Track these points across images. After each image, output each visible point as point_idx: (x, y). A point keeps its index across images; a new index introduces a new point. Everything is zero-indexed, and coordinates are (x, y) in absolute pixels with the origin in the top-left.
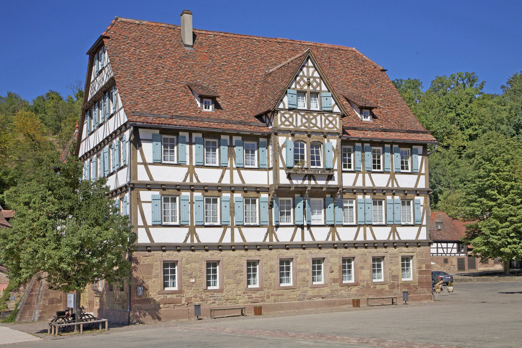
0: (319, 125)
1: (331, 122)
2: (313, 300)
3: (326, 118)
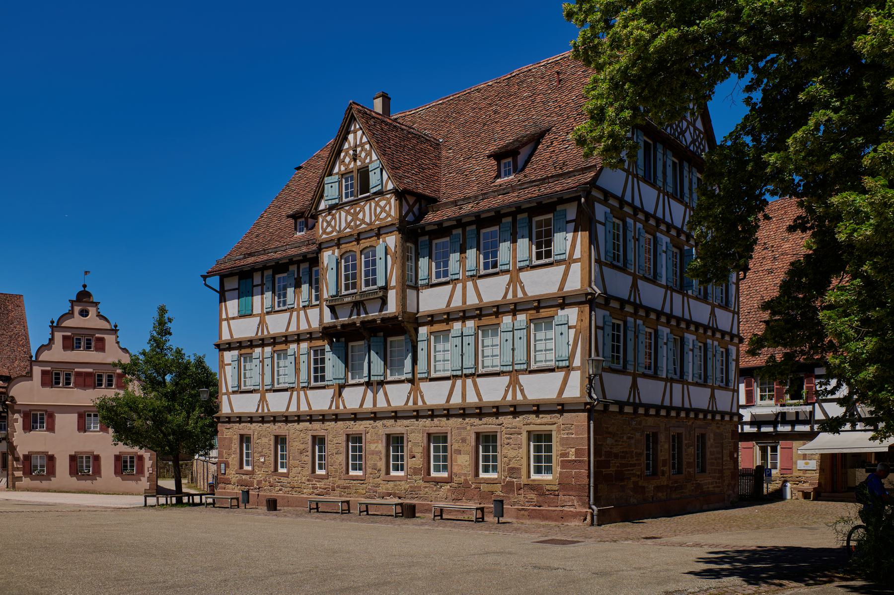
0: (367, 220)
1: (383, 209)
2: (386, 499)
3: (377, 204)
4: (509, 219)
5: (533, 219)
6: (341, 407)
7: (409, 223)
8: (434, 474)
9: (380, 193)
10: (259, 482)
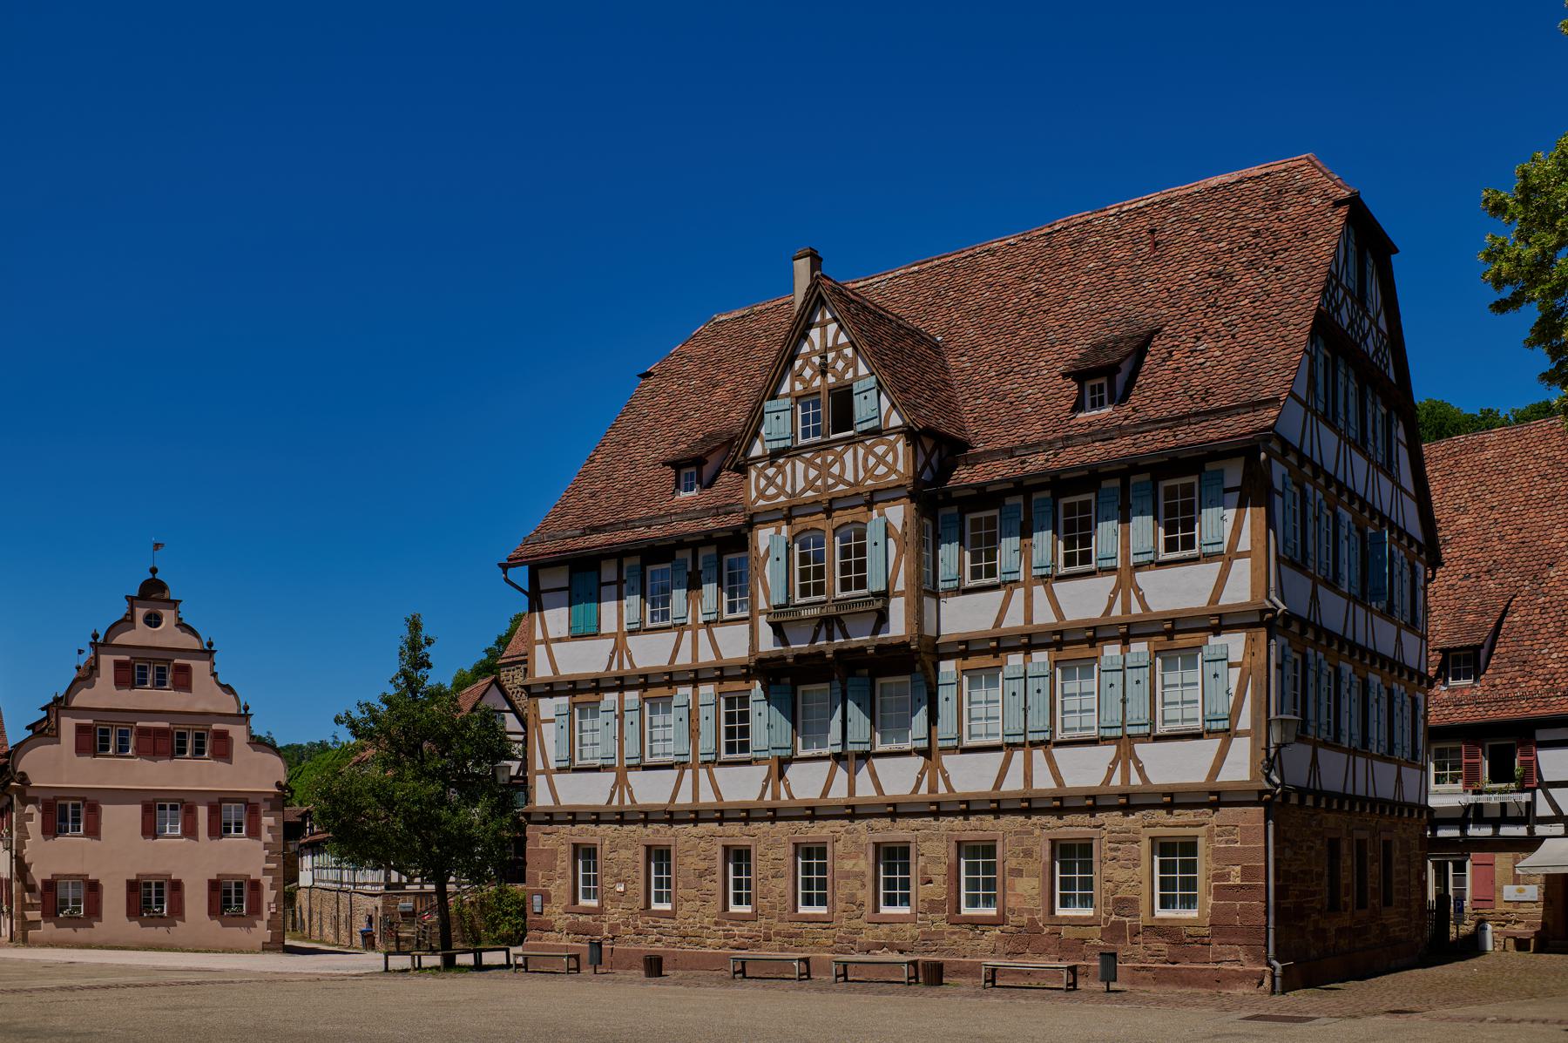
0: (849, 476)
1: (881, 460)
2: (875, 954)
4: (1116, 483)
5: (1160, 483)
6: (784, 796)
7: (927, 484)
8: (966, 911)
9: (877, 432)
10: (613, 928)
